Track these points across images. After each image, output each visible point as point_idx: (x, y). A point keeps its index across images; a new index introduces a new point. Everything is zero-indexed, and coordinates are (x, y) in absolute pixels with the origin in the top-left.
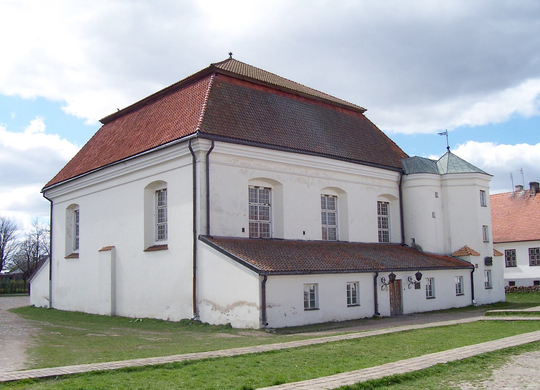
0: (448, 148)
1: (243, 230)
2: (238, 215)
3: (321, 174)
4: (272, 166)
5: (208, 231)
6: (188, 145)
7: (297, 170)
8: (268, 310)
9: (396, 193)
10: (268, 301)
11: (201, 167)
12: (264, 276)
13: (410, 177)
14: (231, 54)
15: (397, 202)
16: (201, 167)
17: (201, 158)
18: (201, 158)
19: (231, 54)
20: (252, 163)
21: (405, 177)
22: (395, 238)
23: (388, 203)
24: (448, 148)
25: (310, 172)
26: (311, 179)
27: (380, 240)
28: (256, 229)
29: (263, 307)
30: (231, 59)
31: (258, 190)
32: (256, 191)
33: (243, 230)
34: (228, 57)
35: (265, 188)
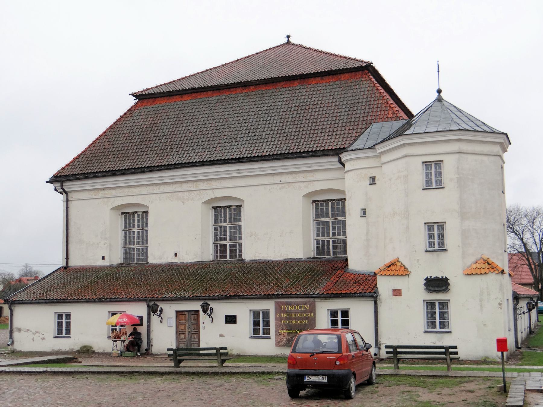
0: (439, 91)
1: (103, 258)
2: (98, 244)
3: (202, 186)
4: (136, 191)
14: (288, 37)
19: (288, 37)
20: (114, 193)
24: (439, 91)
25: (185, 187)
26: (187, 193)
30: (288, 42)
31: (136, 215)
32: (134, 217)
33: (103, 258)
34: (286, 40)
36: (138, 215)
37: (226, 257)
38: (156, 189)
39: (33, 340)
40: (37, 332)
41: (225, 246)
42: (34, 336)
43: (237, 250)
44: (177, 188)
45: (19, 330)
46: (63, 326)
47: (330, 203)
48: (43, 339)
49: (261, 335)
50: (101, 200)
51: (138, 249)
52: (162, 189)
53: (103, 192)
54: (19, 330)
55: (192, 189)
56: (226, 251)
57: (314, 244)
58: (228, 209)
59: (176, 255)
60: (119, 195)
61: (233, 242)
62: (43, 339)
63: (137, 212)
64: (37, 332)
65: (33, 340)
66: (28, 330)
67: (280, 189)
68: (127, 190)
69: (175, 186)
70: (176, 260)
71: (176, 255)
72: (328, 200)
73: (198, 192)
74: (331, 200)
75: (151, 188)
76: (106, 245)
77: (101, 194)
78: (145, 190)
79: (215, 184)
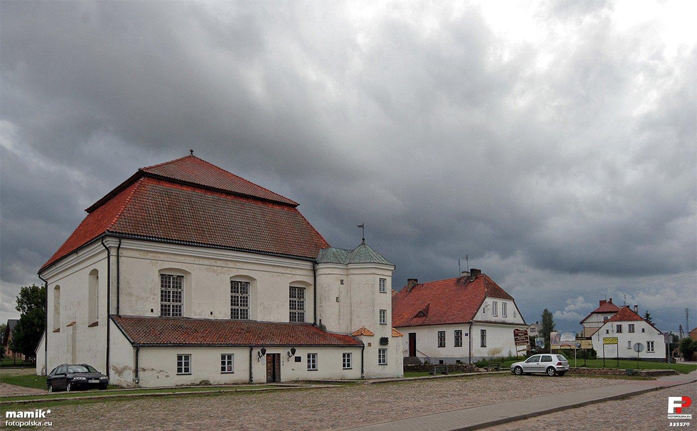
0: (363, 239)
1: (152, 311)
3: (231, 265)
4: (181, 259)
5: (118, 312)
6: (100, 243)
7: (206, 262)
8: (141, 373)
9: (310, 280)
10: (140, 366)
11: (113, 259)
12: (137, 347)
13: (320, 266)
15: (312, 287)
16: (113, 259)
17: (113, 252)
18: (113, 252)
20: (162, 257)
21: (318, 267)
22: (309, 319)
23: (305, 288)
24: (363, 239)
25: (219, 263)
27: (290, 320)
28: (169, 310)
29: (136, 371)
31: (172, 278)
32: (170, 279)
33: (152, 311)
35: (178, 276)
36: (173, 278)
37: (238, 318)
38: (197, 261)
39: (158, 378)
40: (161, 371)
41: (238, 310)
42: (158, 374)
43: (245, 313)
44: (213, 263)
45: (144, 370)
46: (183, 366)
47: (297, 289)
48: (167, 376)
49: (183, 373)
50: (150, 261)
51: (173, 306)
52: (201, 261)
53: (152, 254)
54: (144, 370)
55: (223, 265)
56: (238, 314)
57: (183, 309)
58: (239, 284)
59: (211, 313)
60: (166, 259)
61: (242, 308)
62: (167, 376)
63: (172, 276)
64: (161, 371)
65: (158, 378)
66: (153, 369)
67: (278, 276)
68: (173, 257)
69: (211, 261)
70: (211, 318)
71: (211, 313)
72: (296, 287)
73: (228, 269)
74: (298, 288)
75: (193, 259)
76: (154, 300)
77: (150, 256)
78: (188, 260)
79: (239, 265)
